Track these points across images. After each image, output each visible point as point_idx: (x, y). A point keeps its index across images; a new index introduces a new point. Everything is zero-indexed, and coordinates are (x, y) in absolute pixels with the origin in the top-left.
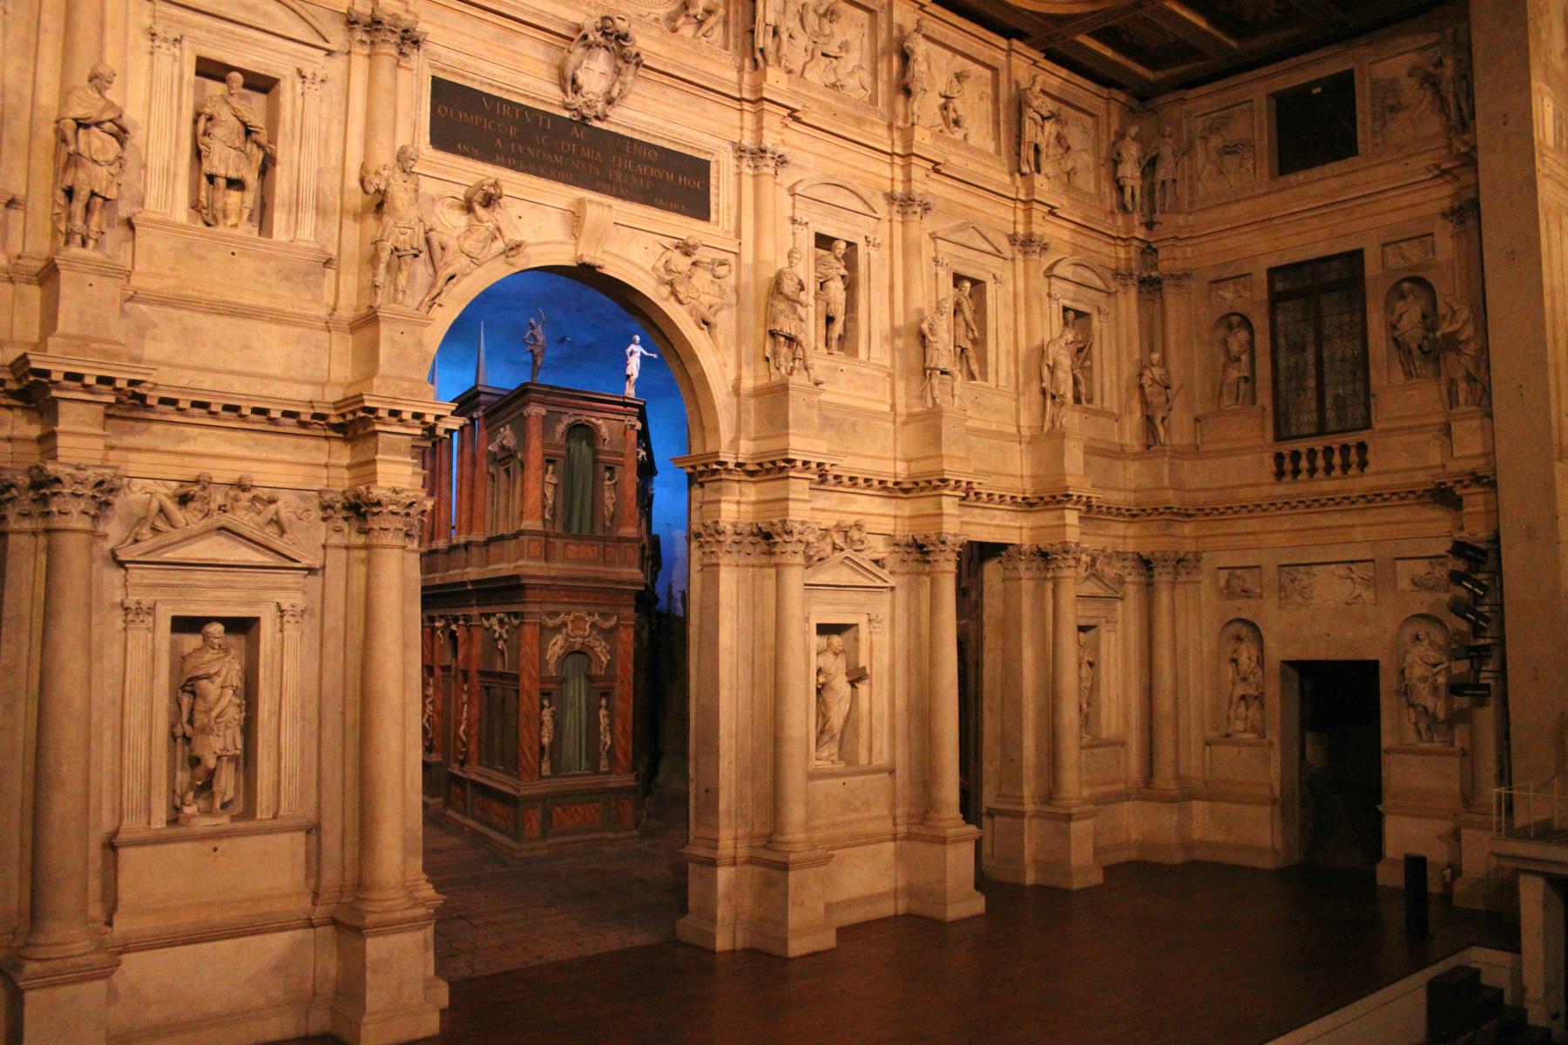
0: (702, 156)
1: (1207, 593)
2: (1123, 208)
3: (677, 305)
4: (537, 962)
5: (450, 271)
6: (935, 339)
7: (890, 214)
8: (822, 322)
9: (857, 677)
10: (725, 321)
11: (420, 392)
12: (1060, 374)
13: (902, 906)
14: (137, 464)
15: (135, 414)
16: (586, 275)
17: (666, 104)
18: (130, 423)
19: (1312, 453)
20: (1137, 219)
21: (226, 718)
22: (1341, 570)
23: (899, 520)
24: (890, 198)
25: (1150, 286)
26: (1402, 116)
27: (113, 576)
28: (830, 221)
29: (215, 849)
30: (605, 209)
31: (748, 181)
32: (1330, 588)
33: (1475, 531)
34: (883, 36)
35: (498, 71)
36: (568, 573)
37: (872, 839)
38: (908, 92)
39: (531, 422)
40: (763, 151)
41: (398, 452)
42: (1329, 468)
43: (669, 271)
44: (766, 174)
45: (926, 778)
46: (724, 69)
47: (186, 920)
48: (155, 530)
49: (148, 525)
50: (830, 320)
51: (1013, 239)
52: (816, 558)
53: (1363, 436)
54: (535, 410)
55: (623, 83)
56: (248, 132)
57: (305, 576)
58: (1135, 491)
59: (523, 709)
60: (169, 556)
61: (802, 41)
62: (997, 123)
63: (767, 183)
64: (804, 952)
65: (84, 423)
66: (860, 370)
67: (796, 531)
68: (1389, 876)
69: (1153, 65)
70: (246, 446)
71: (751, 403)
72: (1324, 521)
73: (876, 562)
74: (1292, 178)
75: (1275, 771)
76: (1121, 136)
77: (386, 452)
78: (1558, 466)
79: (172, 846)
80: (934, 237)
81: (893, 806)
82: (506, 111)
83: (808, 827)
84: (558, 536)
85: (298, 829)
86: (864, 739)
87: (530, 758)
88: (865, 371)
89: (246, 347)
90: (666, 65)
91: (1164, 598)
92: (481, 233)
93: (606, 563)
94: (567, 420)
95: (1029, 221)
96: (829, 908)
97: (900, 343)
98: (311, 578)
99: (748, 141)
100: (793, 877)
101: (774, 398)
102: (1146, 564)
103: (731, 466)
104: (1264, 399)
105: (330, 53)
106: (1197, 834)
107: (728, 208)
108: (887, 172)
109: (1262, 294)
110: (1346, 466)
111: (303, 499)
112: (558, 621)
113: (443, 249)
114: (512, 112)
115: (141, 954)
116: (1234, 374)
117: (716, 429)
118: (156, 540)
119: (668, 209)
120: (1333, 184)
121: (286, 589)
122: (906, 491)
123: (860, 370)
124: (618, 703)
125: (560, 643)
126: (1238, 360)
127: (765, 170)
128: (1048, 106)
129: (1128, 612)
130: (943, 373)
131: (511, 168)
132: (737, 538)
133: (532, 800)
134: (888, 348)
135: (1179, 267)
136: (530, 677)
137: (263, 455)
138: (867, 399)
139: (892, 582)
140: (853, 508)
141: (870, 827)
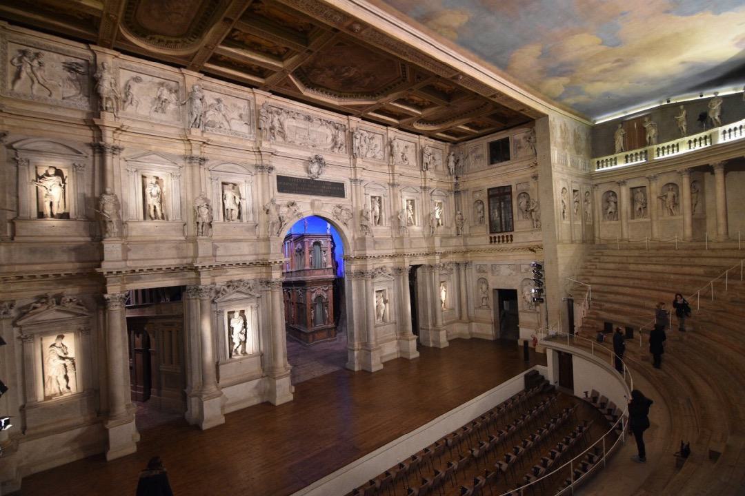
1: (474, 271)
2: (451, 175)
8: (373, 218)
9: (385, 302)
10: (350, 222)
12: (434, 222)
14: (217, 279)
19: (499, 237)
20: (454, 176)
22: (507, 266)
24: (389, 184)
25: (457, 193)
26: (522, 150)
31: (354, 187)
32: (505, 271)
33: (539, 261)
34: (386, 141)
37: (392, 340)
38: (392, 155)
42: (503, 241)
46: (346, 160)
50: (375, 217)
51: (421, 187)
53: (512, 233)
54: (306, 240)
58: (455, 246)
60: (226, 299)
61: (365, 146)
62: (417, 157)
63: (358, 188)
68: (521, 343)
69: (457, 136)
71: (357, 242)
72: (503, 254)
74: (494, 166)
75: (492, 315)
76: (449, 154)
78: (558, 246)
80: (400, 191)
81: (396, 332)
83: (376, 339)
89: (240, 249)
91: (463, 273)
92: (291, 212)
93: (325, 274)
94: (313, 241)
95: (425, 184)
96: (381, 358)
99: (353, 178)
100: (372, 353)
101: (363, 240)
102: (458, 264)
104: (487, 222)
106: (474, 331)
109: (485, 194)
110: (508, 241)
116: (480, 215)
117: (349, 248)
120: (504, 168)
124: (329, 308)
126: (480, 212)
128: (430, 150)
129: (454, 276)
135: (466, 188)
141: (391, 337)
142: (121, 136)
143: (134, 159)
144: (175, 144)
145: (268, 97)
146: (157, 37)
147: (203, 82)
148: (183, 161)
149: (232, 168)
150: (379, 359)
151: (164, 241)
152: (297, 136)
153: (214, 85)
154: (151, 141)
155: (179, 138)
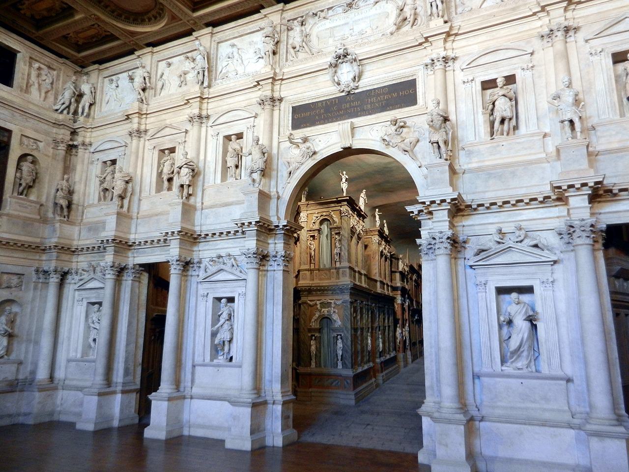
0: (410, 78)
5: (289, 170)
16: (348, 152)
17: (384, 67)
23: (563, 220)
27: (199, 285)
28: (490, 71)
37: (544, 424)
47: (208, 392)
48: (206, 272)
66: (518, 141)
73: (536, 246)
86: (543, 357)
88: (523, 140)
89: (231, 214)
90: (376, 52)
108: (539, 23)
123: (518, 141)
127: (436, 68)
132: (430, 246)
138: (525, 155)
139: (555, 258)
140: (519, 218)
141: (547, 416)
142: (148, 120)
143: (153, 137)
145: (283, 10)
146: (150, 15)
147: (219, 35)
149: (233, 116)
152: (331, 41)
153: (227, 33)
154: (167, 115)
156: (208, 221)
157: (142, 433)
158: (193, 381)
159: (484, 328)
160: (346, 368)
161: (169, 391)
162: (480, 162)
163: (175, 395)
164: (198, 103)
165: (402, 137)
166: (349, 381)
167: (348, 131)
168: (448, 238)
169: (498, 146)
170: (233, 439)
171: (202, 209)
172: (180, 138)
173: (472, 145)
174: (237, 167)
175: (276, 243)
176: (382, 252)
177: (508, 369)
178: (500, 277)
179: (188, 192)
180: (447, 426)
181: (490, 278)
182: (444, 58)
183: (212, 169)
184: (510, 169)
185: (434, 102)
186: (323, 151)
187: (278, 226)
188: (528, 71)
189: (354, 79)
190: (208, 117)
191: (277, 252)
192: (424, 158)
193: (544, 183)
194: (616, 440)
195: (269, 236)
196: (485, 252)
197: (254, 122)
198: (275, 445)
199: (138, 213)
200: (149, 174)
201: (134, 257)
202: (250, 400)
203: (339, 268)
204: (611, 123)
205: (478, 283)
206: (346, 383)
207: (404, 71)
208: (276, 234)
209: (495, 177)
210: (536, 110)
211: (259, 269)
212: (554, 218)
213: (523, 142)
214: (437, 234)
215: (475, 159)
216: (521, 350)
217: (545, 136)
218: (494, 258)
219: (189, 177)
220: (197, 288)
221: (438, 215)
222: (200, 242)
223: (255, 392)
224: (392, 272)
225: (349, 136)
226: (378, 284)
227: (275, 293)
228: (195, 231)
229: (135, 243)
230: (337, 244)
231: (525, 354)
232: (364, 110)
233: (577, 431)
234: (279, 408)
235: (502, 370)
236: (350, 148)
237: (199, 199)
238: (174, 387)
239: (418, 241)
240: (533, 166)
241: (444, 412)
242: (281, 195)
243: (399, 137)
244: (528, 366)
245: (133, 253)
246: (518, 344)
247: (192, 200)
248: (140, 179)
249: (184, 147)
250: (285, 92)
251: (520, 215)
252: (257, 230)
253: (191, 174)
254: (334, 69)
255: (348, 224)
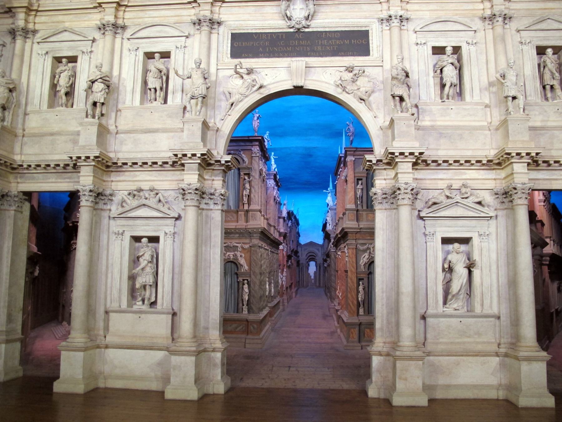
0: (364, 29)
3: (347, 95)
4: (294, 387)
5: (231, 101)
6: (506, 81)
7: (484, 26)
8: (438, 88)
10: (377, 98)
11: (197, 146)
13: (501, 395)
14: (121, 186)
15: (119, 170)
16: (298, 90)
18: (119, 173)
21: (147, 271)
23: (498, 181)
27: (112, 222)
29: (140, 317)
30: (299, 62)
35: (256, 23)
36: (366, 226)
37: (477, 354)
39: (348, 164)
40: (390, 16)
41: (192, 170)
43: (342, 81)
44: (394, 26)
45: (516, 321)
47: (128, 341)
48: (123, 206)
49: (120, 205)
52: (430, 203)
54: (350, 159)
55: (309, 9)
56: (161, 72)
57: (175, 220)
59: (349, 285)
64: (404, 404)
65: (87, 172)
67: (402, 188)
70: (156, 176)
71: (390, 132)
73: (479, 203)
77: (188, 170)
79: (127, 314)
82: (264, 37)
84: (364, 211)
85: (168, 313)
87: (351, 305)
92: (246, 84)
97: (494, 89)
98: (178, 222)
99: (385, 15)
100: (399, 364)
103: (374, 162)
105: (187, 37)
107: (377, 47)
108: (481, 6)
111: (176, 193)
112: (365, 247)
113: (230, 94)
114: (267, 36)
115: (114, 350)
118: (123, 209)
119: (347, 56)
121: (168, 225)
122: (499, 164)
123: (465, 107)
125: (367, 257)
127: (393, 25)
130: (514, 98)
131: (266, 57)
132: (384, 196)
133: (352, 325)
134: (487, 93)
136: (351, 271)
137: (161, 179)
138: (470, 121)
139: (492, 214)
141: (480, 347)
143: (45, 40)
144: (90, 16)
148: (99, 34)
149: (159, 32)
150: (420, 383)
151: (59, 133)
154: (66, 17)
155: (92, 6)
156: (124, 148)
157: (51, 388)
158: (107, 328)
159: (431, 275)
160: (253, 313)
161: (83, 340)
162: (432, 121)
163: (89, 344)
164: (113, 10)
165: (356, 85)
166: (255, 326)
167: (302, 71)
168: (412, 190)
169: (448, 109)
170: (175, 389)
171: (117, 133)
172: (86, 46)
173: (426, 104)
174: (161, 89)
175: (213, 180)
176: (275, 197)
177: (449, 310)
178: (447, 229)
179: (101, 111)
180: (407, 363)
181: (438, 229)
182: (401, 16)
183: (129, 88)
184: (458, 132)
185: (399, 57)
186: (271, 86)
187: (219, 161)
188: (473, 46)
189: (307, 18)
190: (124, 28)
191: (216, 190)
192: (379, 109)
193: (486, 148)
194: (540, 362)
195: (205, 171)
196: (437, 205)
197: (185, 42)
198: (216, 392)
199: (24, 130)
200: (38, 84)
201: (18, 183)
202: (194, 349)
203: (247, 211)
204: (536, 104)
205: (427, 233)
206: (252, 328)
207: (359, 20)
208: (213, 170)
209: (445, 137)
210: (479, 82)
211: (198, 207)
212: (492, 179)
213: (469, 109)
214: (403, 185)
215: (427, 118)
216: (460, 293)
217: (487, 106)
218: (440, 211)
219: (104, 94)
220: (109, 224)
221: (402, 167)
222: (112, 171)
223: (194, 340)
224: (279, 218)
225: (302, 75)
226: (272, 228)
227: (213, 234)
228: (111, 158)
229: (22, 166)
230: (247, 186)
231: (461, 296)
232: (315, 52)
233: (501, 358)
234: (219, 355)
235: (443, 311)
236: (302, 87)
237: (111, 122)
238: (86, 335)
239: (373, 190)
240: (478, 131)
241: (405, 350)
242: (220, 128)
243: (354, 84)
244: (463, 308)
245: (16, 178)
246: (459, 288)
247: (104, 121)
248: (25, 89)
249: (90, 58)
250: (225, 16)
251: (465, 174)
252: (199, 164)
253: (107, 90)
254: (288, 3)
255: (259, 166)
